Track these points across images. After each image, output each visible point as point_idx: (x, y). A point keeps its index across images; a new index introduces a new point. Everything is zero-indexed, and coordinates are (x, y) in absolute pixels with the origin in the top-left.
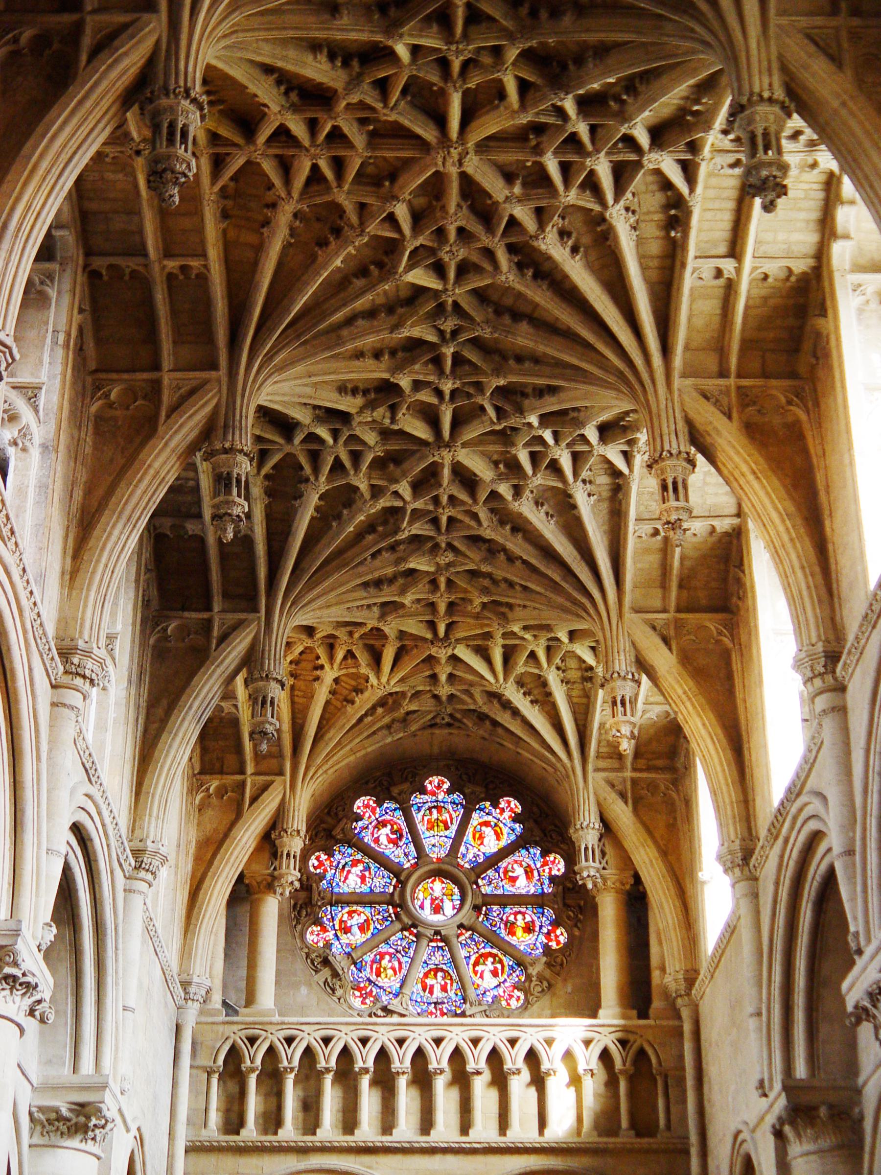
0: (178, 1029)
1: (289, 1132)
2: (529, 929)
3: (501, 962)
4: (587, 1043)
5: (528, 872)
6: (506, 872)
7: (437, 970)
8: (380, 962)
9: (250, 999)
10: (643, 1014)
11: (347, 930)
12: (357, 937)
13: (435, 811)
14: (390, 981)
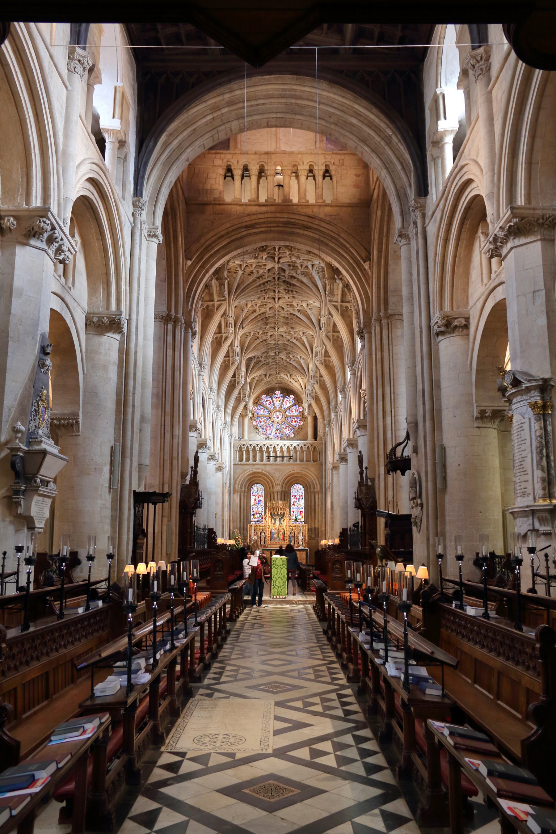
0: (230, 443)
1: (251, 461)
4: (305, 445)
9: (243, 437)
10: (316, 440)
14: (269, 432)
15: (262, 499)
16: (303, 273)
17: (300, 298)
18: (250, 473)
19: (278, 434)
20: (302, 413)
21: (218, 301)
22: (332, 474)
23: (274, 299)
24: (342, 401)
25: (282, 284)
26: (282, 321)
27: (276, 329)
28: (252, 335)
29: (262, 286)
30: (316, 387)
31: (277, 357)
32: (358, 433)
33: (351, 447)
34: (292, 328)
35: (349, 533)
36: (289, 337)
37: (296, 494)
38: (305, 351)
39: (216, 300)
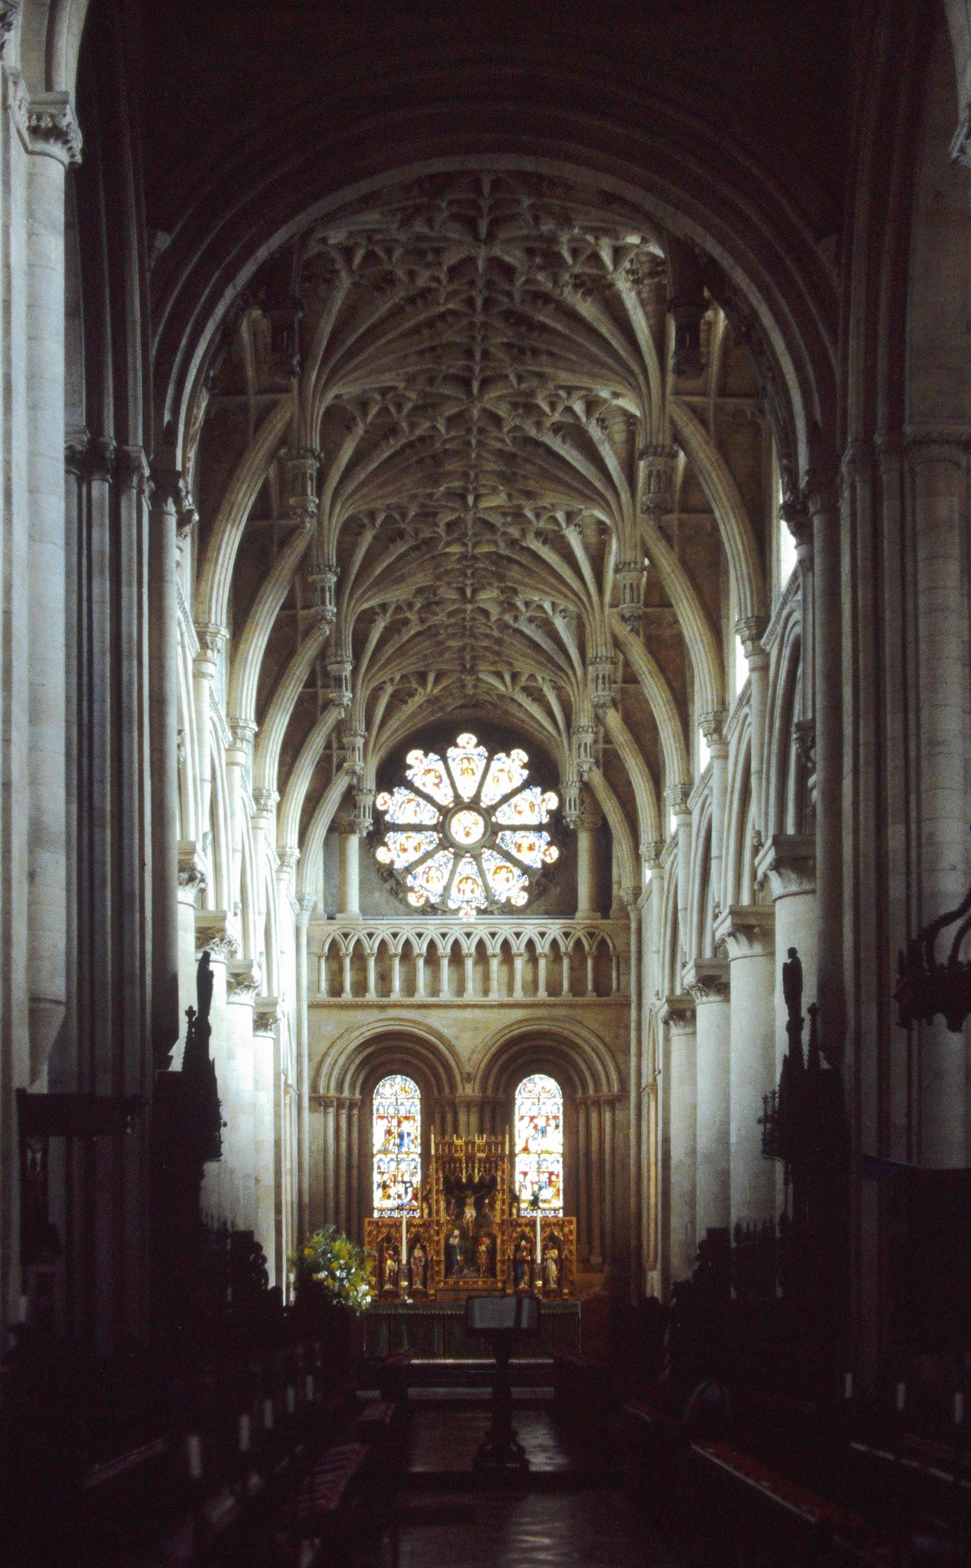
2: (531, 848)
3: (511, 871)
5: (532, 806)
6: (516, 807)
7: (467, 878)
8: (428, 873)
11: (405, 850)
12: (413, 856)
13: (465, 761)
15: (413, 1128)
16: (579, 283)
17: (565, 378)
18: (368, 1034)
19: (468, 896)
20: (557, 816)
21: (259, 392)
22: (667, 1039)
23: (466, 383)
24: (709, 769)
25: (499, 324)
26: (491, 466)
27: (470, 499)
28: (379, 522)
29: (426, 332)
30: (613, 719)
31: (469, 607)
32: (776, 885)
33: (743, 939)
34: (529, 495)
35: (734, 1245)
36: (514, 532)
37: (534, 1113)
38: (575, 584)
39: (251, 388)
